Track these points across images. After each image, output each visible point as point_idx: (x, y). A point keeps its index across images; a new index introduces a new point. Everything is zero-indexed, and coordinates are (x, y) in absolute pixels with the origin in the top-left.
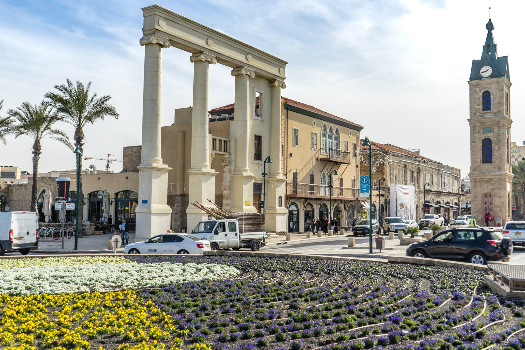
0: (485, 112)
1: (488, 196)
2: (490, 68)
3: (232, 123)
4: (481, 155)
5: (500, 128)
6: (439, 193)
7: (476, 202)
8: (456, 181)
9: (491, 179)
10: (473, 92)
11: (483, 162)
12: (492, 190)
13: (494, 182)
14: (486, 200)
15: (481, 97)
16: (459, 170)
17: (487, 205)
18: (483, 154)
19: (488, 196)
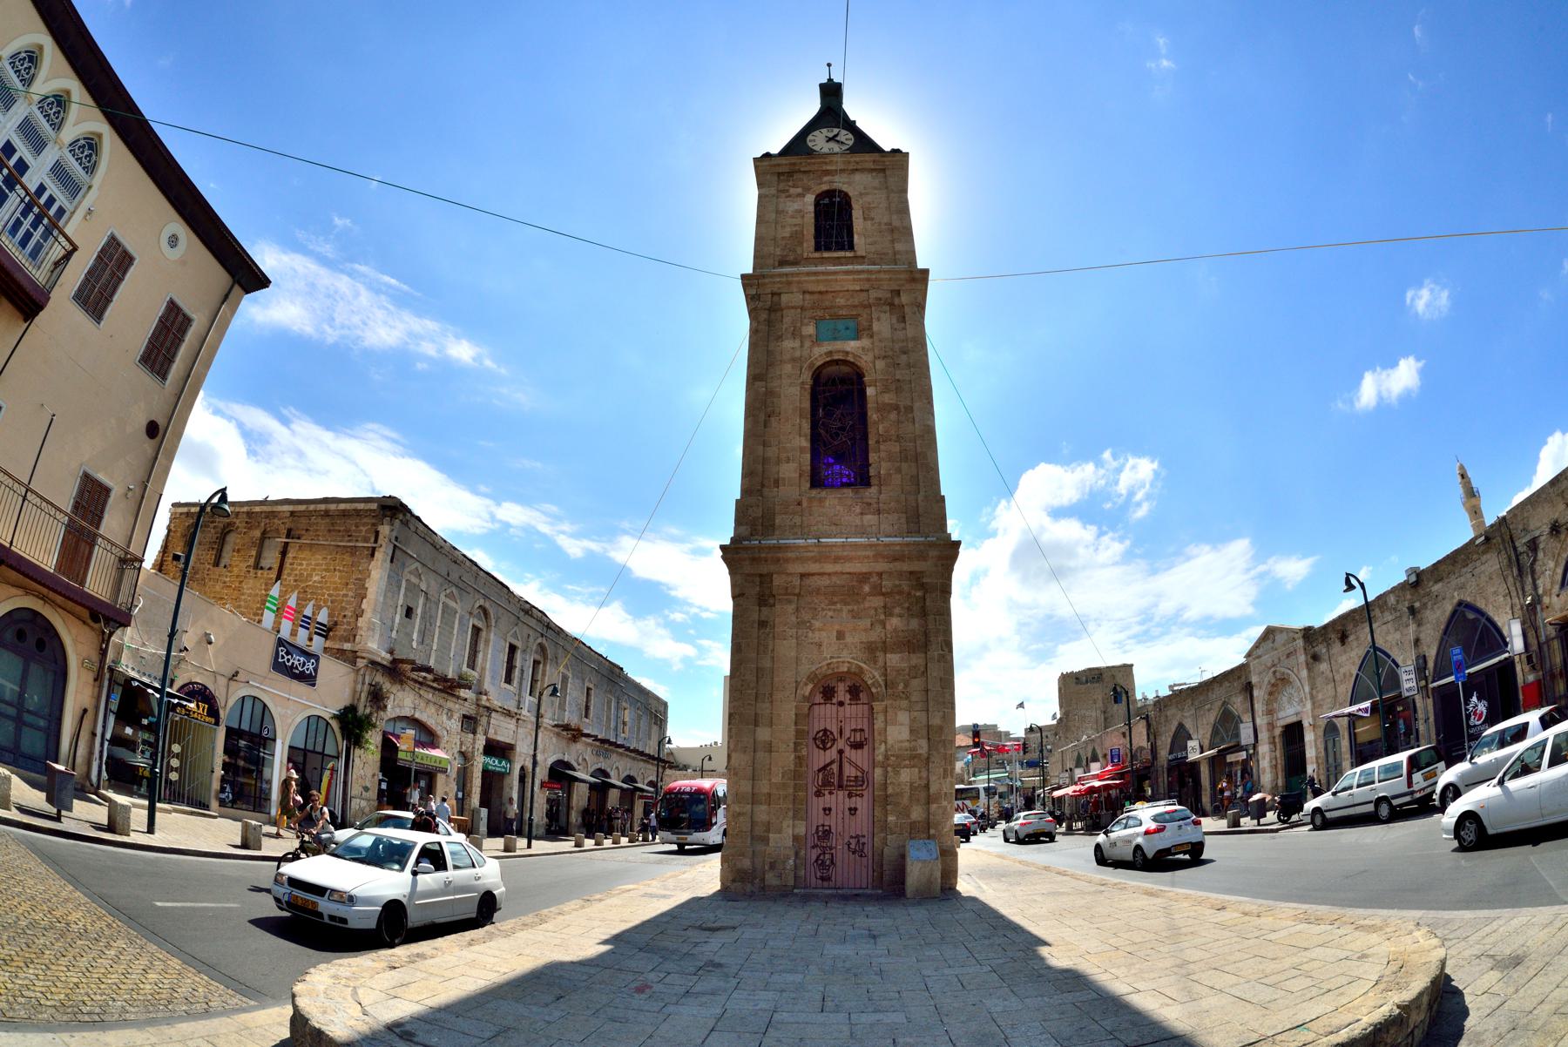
0: (826, 255)
1: (842, 693)
4: (806, 444)
5: (903, 319)
6: (606, 745)
7: (763, 734)
8: (655, 728)
9: (864, 577)
10: (773, 191)
11: (816, 482)
12: (871, 650)
13: (878, 602)
14: (826, 717)
15: (812, 208)
16: (665, 705)
17: (832, 754)
18: (815, 439)
19: (842, 693)
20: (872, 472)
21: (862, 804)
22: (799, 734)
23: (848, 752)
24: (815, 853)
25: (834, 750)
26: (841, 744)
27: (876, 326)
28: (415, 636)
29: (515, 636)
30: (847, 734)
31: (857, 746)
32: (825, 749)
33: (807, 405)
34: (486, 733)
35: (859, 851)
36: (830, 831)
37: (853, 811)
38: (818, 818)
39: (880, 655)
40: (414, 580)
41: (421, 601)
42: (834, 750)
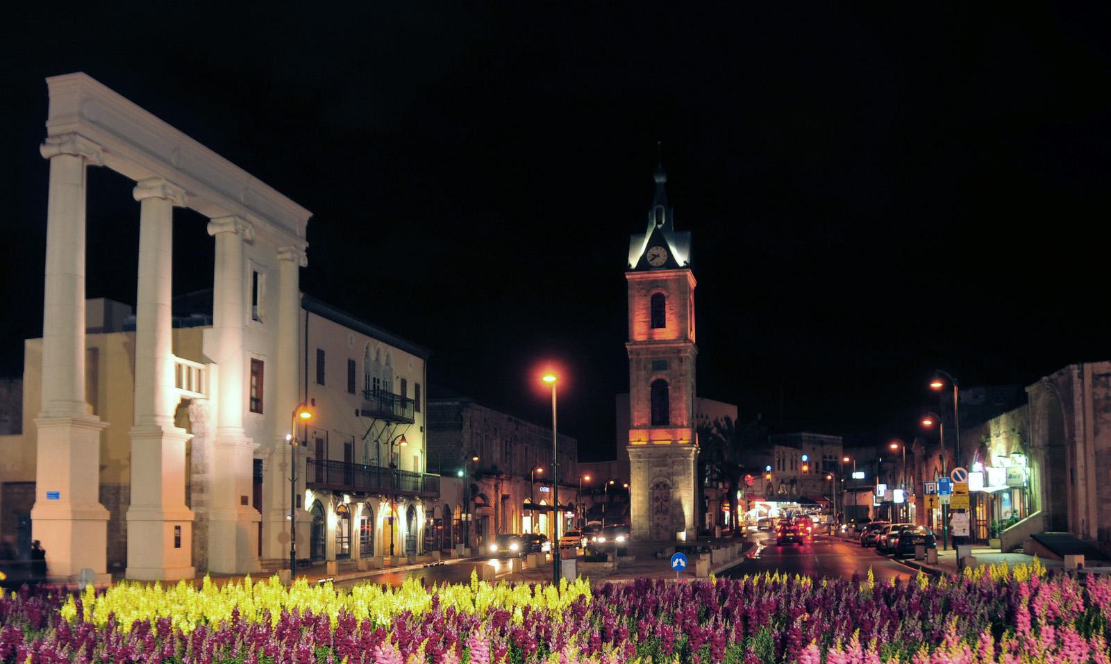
1: (661, 487)
2: (663, 250)
3: (207, 332)
4: (650, 411)
9: (667, 455)
14: (657, 493)
19: (661, 487)
20: (670, 420)
23: (664, 503)
26: (661, 500)
27: (672, 365)
30: (663, 498)
31: (666, 501)
32: (657, 501)
33: (650, 396)
35: (667, 530)
37: (665, 519)
38: (656, 521)
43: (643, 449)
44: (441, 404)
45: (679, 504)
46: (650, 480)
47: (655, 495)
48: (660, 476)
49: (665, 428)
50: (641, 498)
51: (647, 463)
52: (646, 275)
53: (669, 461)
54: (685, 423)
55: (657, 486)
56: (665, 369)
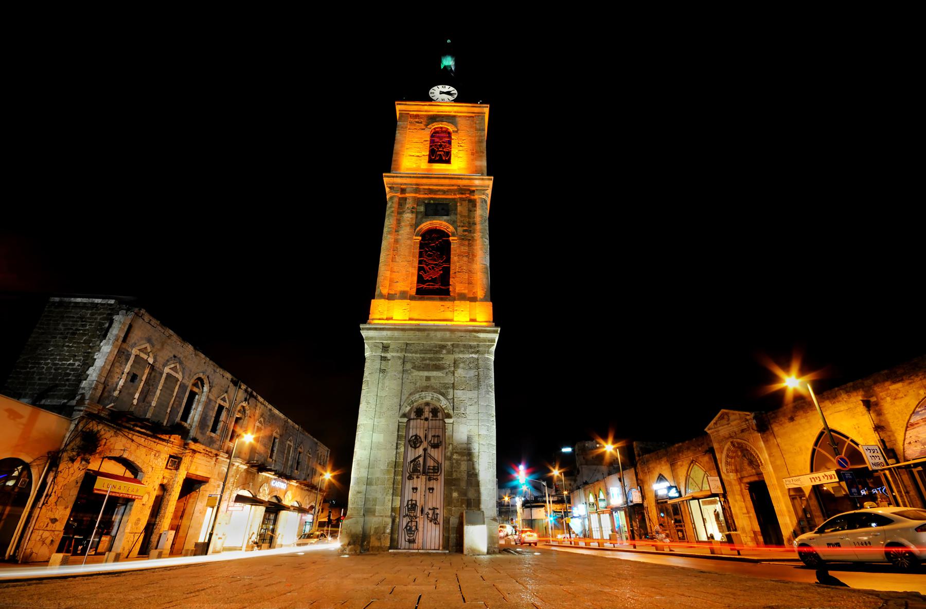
1: (427, 413)
4: (416, 272)
14: (417, 428)
17: (420, 451)
19: (427, 413)
21: (439, 486)
22: (399, 437)
24: (405, 521)
25: (421, 449)
26: (425, 445)
28: (137, 396)
29: (224, 400)
31: (435, 446)
32: (415, 448)
34: (187, 470)
35: (434, 520)
36: (416, 505)
38: (408, 495)
39: (451, 391)
40: (143, 356)
41: (147, 371)
42: (421, 449)
43: (396, 334)
44: (85, 300)
45: (467, 453)
46: (404, 398)
47: (412, 433)
48: (426, 389)
49: (441, 299)
50: (379, 438)
51: (400, 362)
52: (426, 108)
53: (448, 359)
54: (480, 294)
55: (419, 412)
56: (447, 215)
